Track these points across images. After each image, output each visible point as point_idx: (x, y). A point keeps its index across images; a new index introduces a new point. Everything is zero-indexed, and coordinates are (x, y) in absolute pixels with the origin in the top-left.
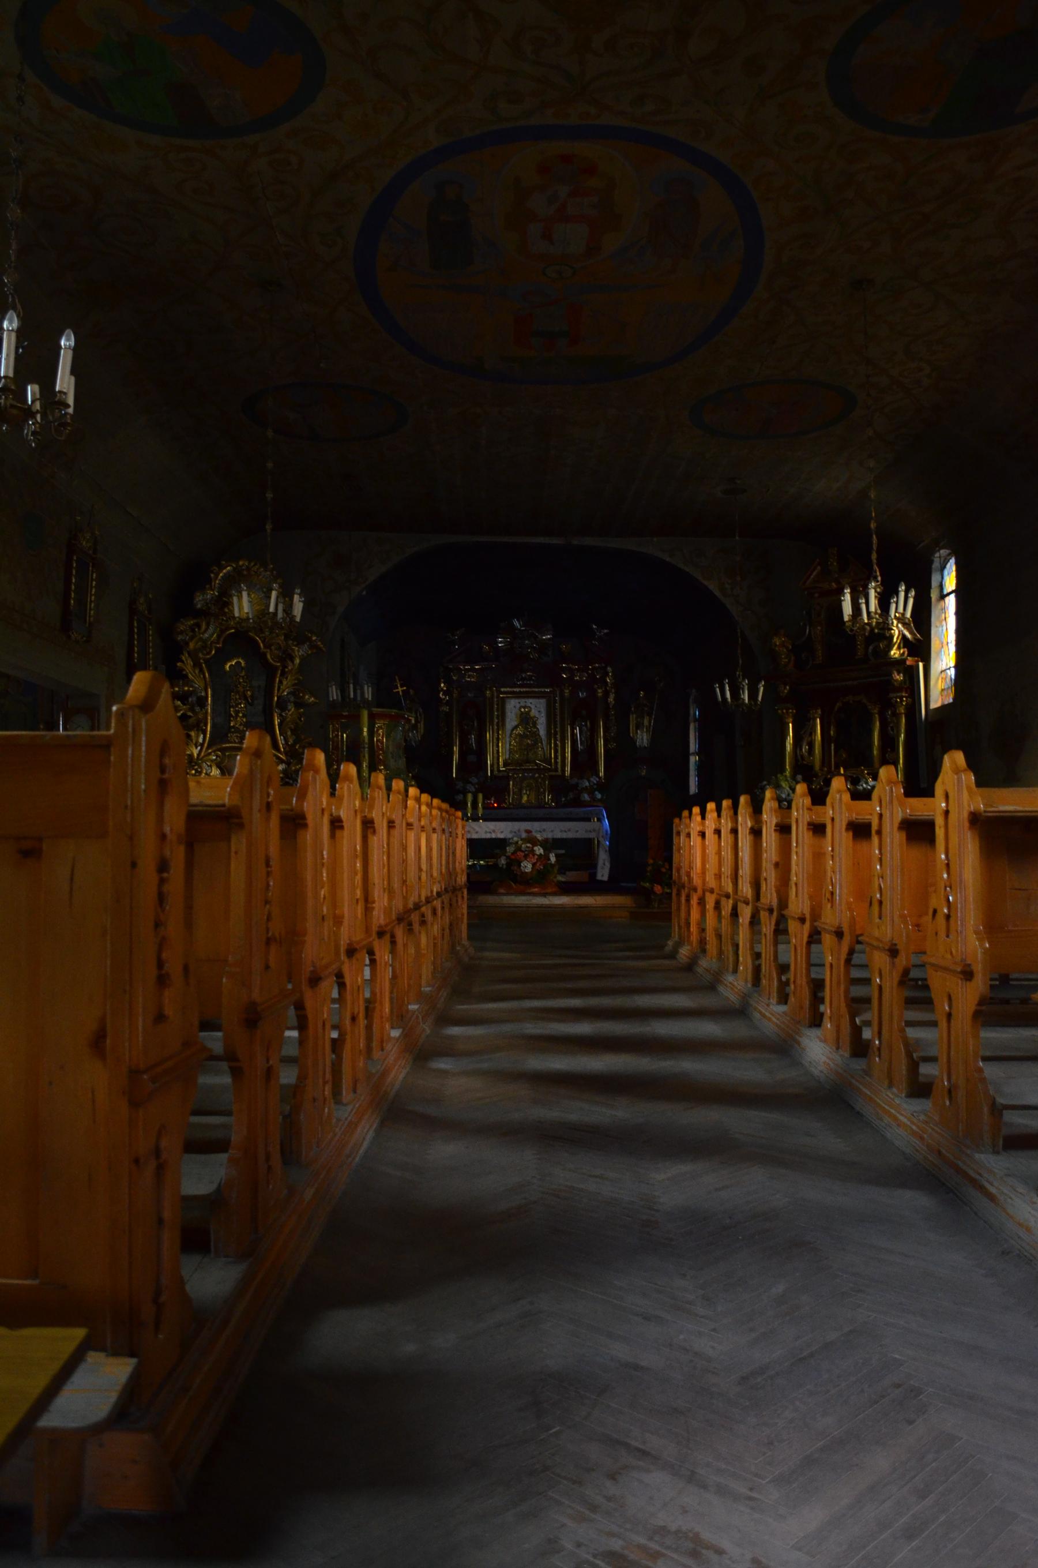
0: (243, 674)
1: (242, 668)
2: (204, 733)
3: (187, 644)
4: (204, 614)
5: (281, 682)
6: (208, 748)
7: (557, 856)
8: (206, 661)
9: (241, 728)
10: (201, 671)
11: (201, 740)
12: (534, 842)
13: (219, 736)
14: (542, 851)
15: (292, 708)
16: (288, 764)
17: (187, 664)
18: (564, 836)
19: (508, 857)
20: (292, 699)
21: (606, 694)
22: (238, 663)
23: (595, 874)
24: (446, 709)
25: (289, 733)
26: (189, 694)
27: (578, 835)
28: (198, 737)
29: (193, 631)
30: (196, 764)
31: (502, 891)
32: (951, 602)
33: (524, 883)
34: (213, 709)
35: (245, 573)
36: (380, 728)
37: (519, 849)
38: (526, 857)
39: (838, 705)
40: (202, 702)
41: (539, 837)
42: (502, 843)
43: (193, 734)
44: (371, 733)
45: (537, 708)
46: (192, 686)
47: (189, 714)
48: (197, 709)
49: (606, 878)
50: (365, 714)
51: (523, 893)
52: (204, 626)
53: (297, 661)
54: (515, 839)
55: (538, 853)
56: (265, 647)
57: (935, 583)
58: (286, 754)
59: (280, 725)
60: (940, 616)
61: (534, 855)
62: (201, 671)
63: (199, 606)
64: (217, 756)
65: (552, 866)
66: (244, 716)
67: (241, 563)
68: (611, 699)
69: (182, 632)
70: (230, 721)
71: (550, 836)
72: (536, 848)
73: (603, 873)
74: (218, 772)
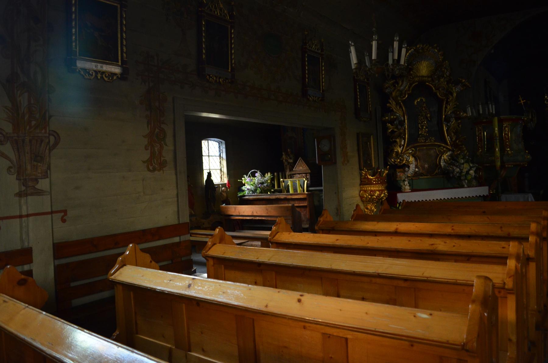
0: (425, 105)
1: (424, 102)
2: (404, 139)
3: (391, 93)
5: (446, 107)
6: (406, 147)
8: (404, 102)
9: (425, 134)
10: (401, 107)
11: (403, 143)
13: (413, 141)
15: (453, 121)
16: (453, 151)
17: (392, 104)
20: (453, 116)
22: (421, 100)
25: (453, 134)
26: (395, 119)
28: (401, 142)
29: (395, 86)
30: (400, 156)
36: (506, 127)
40: (402, 123)
43: (398, 140)
44: (501, 130)
46: (396, 115)
47: (396, 130)
48: (399, 127)
50: (496, 120)
52: (400, 84)
53: (455, 94)
56: (436, 89)
59: (447, 131)
62: (401, 107)
64: (412, 151)
69: (387, 88)
70: (419, 131)
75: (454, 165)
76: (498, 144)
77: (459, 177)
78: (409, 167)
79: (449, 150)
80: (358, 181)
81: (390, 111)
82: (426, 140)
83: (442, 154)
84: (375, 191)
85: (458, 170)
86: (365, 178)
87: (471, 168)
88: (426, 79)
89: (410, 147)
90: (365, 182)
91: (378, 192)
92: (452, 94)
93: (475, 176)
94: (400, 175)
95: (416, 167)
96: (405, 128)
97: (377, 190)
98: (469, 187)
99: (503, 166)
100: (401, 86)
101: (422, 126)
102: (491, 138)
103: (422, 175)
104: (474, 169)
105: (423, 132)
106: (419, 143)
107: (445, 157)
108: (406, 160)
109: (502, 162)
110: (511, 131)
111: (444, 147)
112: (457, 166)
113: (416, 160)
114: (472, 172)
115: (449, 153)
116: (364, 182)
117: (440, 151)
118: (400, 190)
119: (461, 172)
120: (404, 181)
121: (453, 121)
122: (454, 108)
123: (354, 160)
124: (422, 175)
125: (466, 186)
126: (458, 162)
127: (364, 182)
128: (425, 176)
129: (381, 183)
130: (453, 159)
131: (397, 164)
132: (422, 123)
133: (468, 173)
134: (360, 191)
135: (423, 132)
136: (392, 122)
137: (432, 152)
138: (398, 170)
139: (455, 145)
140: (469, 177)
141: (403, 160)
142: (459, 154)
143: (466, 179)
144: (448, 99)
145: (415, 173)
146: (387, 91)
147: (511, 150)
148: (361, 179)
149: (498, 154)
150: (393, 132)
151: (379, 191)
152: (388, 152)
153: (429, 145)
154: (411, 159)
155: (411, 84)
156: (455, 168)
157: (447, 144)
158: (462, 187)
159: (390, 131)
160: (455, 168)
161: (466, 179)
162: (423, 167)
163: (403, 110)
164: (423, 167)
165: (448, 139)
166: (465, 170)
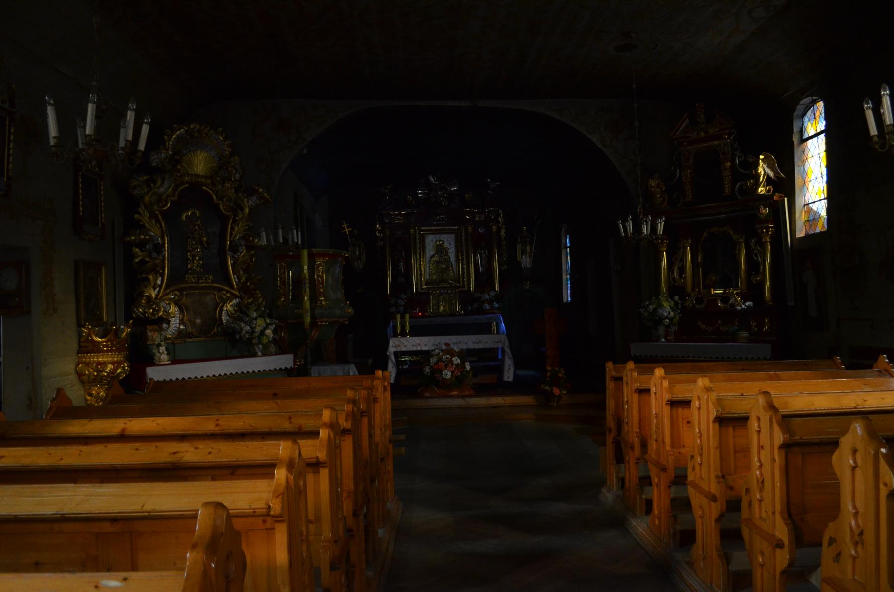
0: (199, 223)
2: (162, 275)
5: (233, 229)
6: (166, 288)
9: (198, 269)
10: (158, 221)
11: (159, 282)
12: (452, 353)
13: (176, 280)
14: (459, 361)
15: (243, 251)
16: (242, 298)
17: (144, 216)
18: (476, 346)
19: (431, 367)
20: (243, 242)
21: (499, 230)
23: (502, 378)
24: (382, 244)
25: (242, 272)
27: (487, 346)
28: (156, 279)
30: (154, 303)
31: (427, 395)
33: (446, 388)
35: (196, 134)
36: (320, 265)
37: (440, 360)
38: (446, 365)
39: (705, 234)
40: (159, 249)
42: (427, 354)
43: (151, 277)
44: (312, 269)
45: (449, 242)
47: (147, 259)
48: (154, 255)
49: (511, 380)
51: (445, 396)
52: (159, 183)
53: (247, 210)
54: (437, 351)
55: (455, 362)
57: (796, 129)
58: (239, 291)
59: (233, 266)
60: (800, 157)
61: (453, 364)
62: (158, 221)
63: (154, 164)
65: (468, 372)
66: (200, 259)
67: (192, 126)
68: (502, 233)
69: (135, 187)
70: (187, 264)
71: (465, 347)
72: (454, 359)
73: (508, 375)
75: (242, 321)
76: (308, 290)
77: (250, 340)
78: (169, 323)
79: (236, 297)
80: (75, 346)
81: (139, 226)
82: (199, 278)
83: (225, 302)
84: (105, 364)
85: (248, 328)
86: (87, 340)
87: (268, 325)
88: (203, 180)
89: (172, 289)
92: (242, 210)
93: (274, 339)
94: (154, 336)
95: (182, 322)
96: (164, 257)
97: (111, 362)
98: (264, 355)
99: (314, 324)
100: (161, 185)
101: (194, 257)
102: (298, 281)
103: (190, 335)
104: (273, 327)
105: (195, 264)
107: (229, 307)
108: (165, 311)
109: (313, 317)
110: (327, 272)
111: (228, 292)
112: (246, 323)
113: (181, 311)
114: (269, 332)
115: (235, 302)
116: (86, 347)
117: (221, 299)
118: (152, 361)
119: (253, 332)
120: (159, 345)
121: (243, 251)
122: (246, 230)
124: (190, 335)
125: (260, 353)
126: (248, 316)
127: (86, 347)
128: (196, 337)
130: (242, 311)
133: (262, 333)
135: (195, 264)
136: (141, 245)
137: (208, 299)
138: (149, 327)
140: (265, 340)
141: (159, 311)
142: (251, 304)
143: (259, 343)
145: (180, 332)
146: (135, 192)
147: (326, 300)
148: (80, 342)
149: (307, 305)
150: (142, 262)
151: (113, 363)
152: (133, 296)
153: (202, 288)
154: (173, 309)
155: (177, 186)
156: (243, 325)
157: (232, 286)
158: (254, 355)
159: (137, 260)
160: (243, 325)
162: (193, 324)
164: (193, 324)
165: (234, 279)
166: (258, 329)
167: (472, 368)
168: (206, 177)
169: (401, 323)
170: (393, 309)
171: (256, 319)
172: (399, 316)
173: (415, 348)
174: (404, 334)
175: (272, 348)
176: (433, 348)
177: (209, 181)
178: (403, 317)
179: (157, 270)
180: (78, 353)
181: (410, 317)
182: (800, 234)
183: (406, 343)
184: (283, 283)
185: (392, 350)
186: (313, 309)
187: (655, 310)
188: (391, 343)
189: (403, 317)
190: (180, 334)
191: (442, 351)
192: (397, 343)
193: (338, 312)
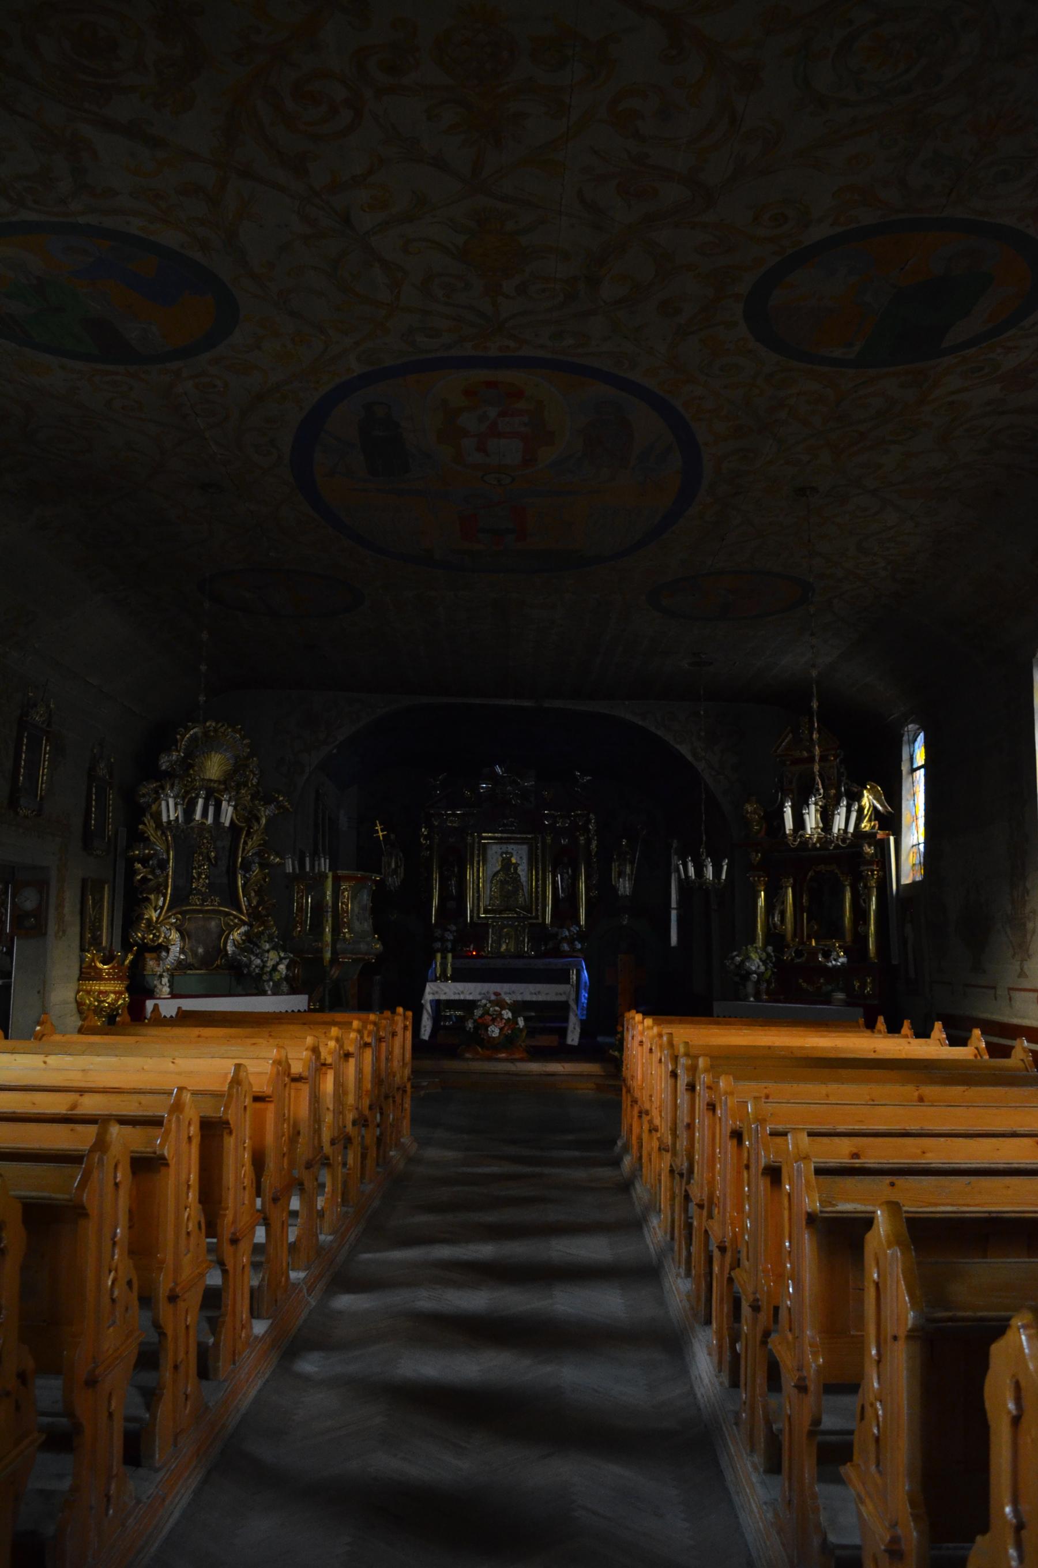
2: (165, 896)
3: (150, 806)
4: (170, 775)
5: (245, 843)
6: (168, 910)
7: (526, 1019)
9: (203, 889)
11: (160, 903)
12: (501, 1004)
13: (179, 900)
14: (510, 1015)
16: (251, 925)
18: (534, 998)
20: (257, 860)
25: (253, 894)
26: (150, 857)
27: (549, 998)
28: (157, 900)
30: (155, 928)
32: (920, 775)
34: (174, 872)
36: (345, 890)
38: (494, 1020)
40: (163, 865)
41: (508, 1000)
42: (469, 1006)
43: (152, 897)
47: (150, 877)
48: (158, 872)
49: (576, 1042)
51: (490, 1059)
53: (264, 821)
54: (484, 1002)
55: (505, 1017)
58: (249, 915)
59: (244, 886)
61: (502, 1019)
63: (164, 768)
64: (177, 919)
65: (521, 1030)
66: (206, 878)
67: (208, 724)
71: (519, 998)
72: (503, 1012)
73: (573, 1038)
74: (177, 935)
75: (252, 953)
76: (330, 919)
78: (168, 951)
79: (244, 923)
80: (76, 973)
82: (204, 900)
83: (231, 929)
84: (106, 993)
85: (259, 961)
86: (90, 967)
87: (281, 959)
90: (89, 973)
91: (112, 995)
92: (258, 820)
93: (287, 975)
94: (151, 963)
95: (182, 951)
96: (168, 875)
97: (111, 992)
98: (274, 994)
99: (334, 960)
101: (199, 874)
102: (319, 908)
103: (190, 966)
105: (200, 884)
106: (190, 904)
107: (236, 935)
108: (165, 937)
109: (334, 952)
110: (354, 898)
111: (235, 917)
112: (257, 955)
113: (182, 937)
114: (282, 967)
115: (243, 929)
116: (88, 973)
117: (227, 925)
118: (151, 994)
119: (264, 966)
120: (161, 976)
122: (260, 845)
123: (74, 930)
124: (190, 966)
126: (259, 947)
127: (88, 973)
129: (119, 978)
130: (251, 941)
131: (146, 944)
132: (200, 867)
133: (275, 968)
134: (78, 992)
135: (200, 884)
136: (144, 861)
138: (148, 955)
139: (255, 915)
140: (276, 976)
141: (159, 937)
142: (262, 933)
143: (271, 979)
144: (250, 827)
145: (180, 962)
146: (142, 800)
147: (350, 932)
148: (81, 968)
149: (328, 937)
150: (144, 880)
151: (115, 993)
152: (131, 918)
154: (174, 936)
156: (253, 958)
157: (240, 911)
158: (264, 993)
159: (139, 877)
160: (253, 958)
161: (271, 979)
162: (195, 954)
163: (167, 839)
164: (195, 954)
165: (243, 901)
166: (270, 964)
167: (526, 1026)
168: (219, 782)
169: (441, 964)
170: (438, 945)
171: (268, 951)
172: (439, 956)
173: (457, 997)
174: (443, 978)
175: (285, 987)
176: (479, 997)
177: (222, 787)
178: (444, 958)
179: (160, 890)
180: (79, 980)
181: (453, 958)
182: (906, 880)
183: (446, 990)
184: (300, 909)
185: (428, 997)
186: (334, 942)
187: (743, 962)
188: (428, 989)
189: (444, 958)
190: (180, 966)
191: (490, 1002)
192: (436, 989)
193: (363, 947)
